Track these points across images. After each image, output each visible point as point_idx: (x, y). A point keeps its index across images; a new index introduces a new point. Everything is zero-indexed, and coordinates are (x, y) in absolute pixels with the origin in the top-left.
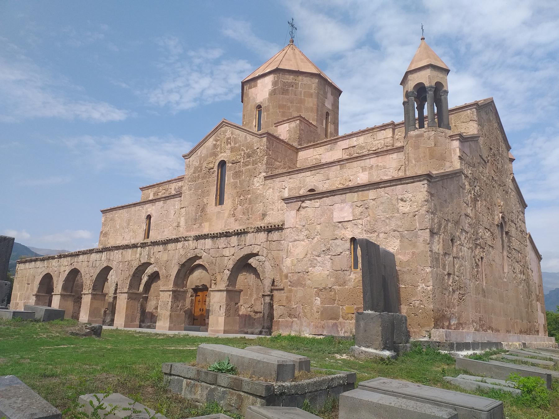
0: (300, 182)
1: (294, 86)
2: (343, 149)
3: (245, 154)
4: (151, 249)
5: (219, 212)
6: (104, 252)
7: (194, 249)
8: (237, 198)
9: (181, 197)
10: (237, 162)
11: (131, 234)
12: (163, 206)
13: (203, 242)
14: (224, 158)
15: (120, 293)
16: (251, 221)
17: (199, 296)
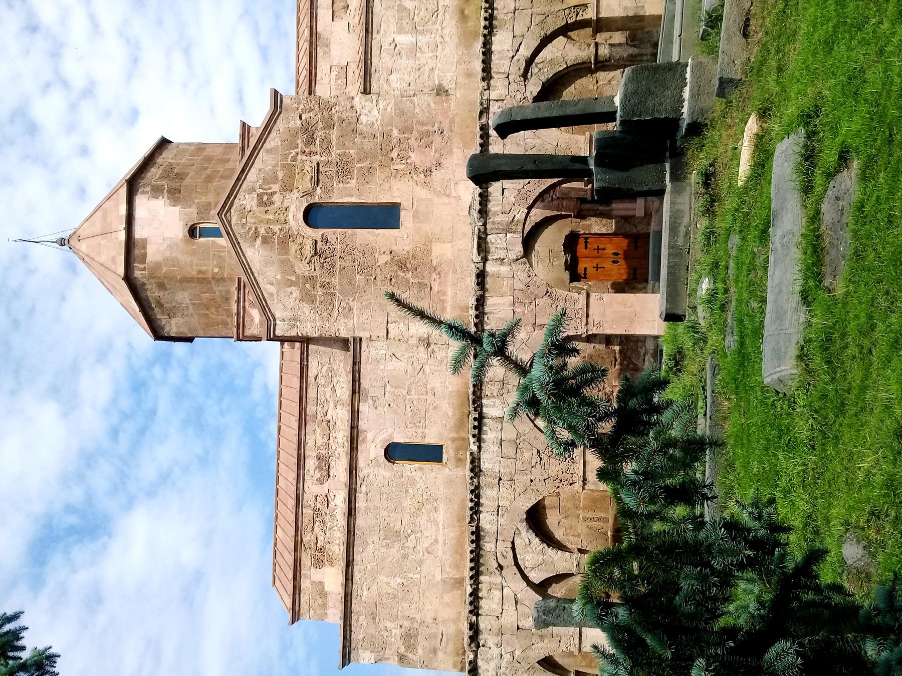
0: (390, 7)
1: (173, 167)
2: (333, 21)
3: (305, 152)
4: (493, 223)
5: (416, 216)
6: (482, 410)
7: (509, 84)
8: (393, 165)
9: (361, 340)
10: (316, 168)
11: (423, 519)
12: (370, 401)
13: (496, 56)
14: (300, 210)
15: (587, 324)
16: (446, 126)
17: (585, 269)
